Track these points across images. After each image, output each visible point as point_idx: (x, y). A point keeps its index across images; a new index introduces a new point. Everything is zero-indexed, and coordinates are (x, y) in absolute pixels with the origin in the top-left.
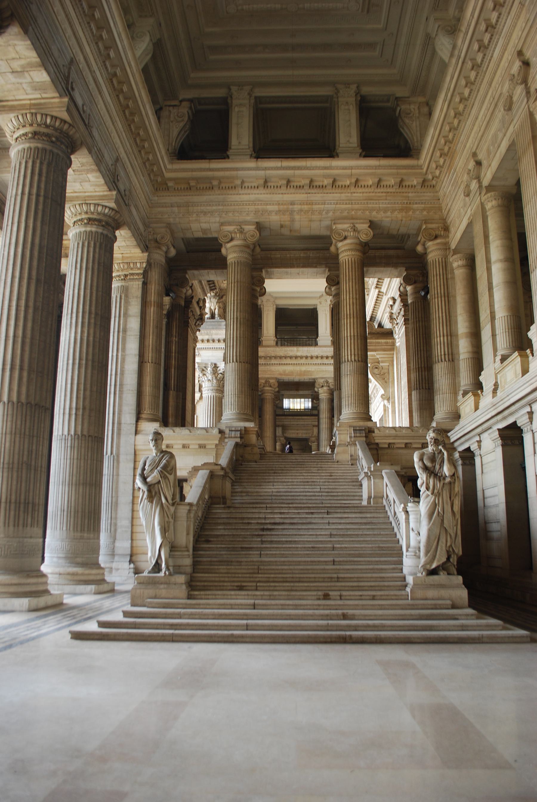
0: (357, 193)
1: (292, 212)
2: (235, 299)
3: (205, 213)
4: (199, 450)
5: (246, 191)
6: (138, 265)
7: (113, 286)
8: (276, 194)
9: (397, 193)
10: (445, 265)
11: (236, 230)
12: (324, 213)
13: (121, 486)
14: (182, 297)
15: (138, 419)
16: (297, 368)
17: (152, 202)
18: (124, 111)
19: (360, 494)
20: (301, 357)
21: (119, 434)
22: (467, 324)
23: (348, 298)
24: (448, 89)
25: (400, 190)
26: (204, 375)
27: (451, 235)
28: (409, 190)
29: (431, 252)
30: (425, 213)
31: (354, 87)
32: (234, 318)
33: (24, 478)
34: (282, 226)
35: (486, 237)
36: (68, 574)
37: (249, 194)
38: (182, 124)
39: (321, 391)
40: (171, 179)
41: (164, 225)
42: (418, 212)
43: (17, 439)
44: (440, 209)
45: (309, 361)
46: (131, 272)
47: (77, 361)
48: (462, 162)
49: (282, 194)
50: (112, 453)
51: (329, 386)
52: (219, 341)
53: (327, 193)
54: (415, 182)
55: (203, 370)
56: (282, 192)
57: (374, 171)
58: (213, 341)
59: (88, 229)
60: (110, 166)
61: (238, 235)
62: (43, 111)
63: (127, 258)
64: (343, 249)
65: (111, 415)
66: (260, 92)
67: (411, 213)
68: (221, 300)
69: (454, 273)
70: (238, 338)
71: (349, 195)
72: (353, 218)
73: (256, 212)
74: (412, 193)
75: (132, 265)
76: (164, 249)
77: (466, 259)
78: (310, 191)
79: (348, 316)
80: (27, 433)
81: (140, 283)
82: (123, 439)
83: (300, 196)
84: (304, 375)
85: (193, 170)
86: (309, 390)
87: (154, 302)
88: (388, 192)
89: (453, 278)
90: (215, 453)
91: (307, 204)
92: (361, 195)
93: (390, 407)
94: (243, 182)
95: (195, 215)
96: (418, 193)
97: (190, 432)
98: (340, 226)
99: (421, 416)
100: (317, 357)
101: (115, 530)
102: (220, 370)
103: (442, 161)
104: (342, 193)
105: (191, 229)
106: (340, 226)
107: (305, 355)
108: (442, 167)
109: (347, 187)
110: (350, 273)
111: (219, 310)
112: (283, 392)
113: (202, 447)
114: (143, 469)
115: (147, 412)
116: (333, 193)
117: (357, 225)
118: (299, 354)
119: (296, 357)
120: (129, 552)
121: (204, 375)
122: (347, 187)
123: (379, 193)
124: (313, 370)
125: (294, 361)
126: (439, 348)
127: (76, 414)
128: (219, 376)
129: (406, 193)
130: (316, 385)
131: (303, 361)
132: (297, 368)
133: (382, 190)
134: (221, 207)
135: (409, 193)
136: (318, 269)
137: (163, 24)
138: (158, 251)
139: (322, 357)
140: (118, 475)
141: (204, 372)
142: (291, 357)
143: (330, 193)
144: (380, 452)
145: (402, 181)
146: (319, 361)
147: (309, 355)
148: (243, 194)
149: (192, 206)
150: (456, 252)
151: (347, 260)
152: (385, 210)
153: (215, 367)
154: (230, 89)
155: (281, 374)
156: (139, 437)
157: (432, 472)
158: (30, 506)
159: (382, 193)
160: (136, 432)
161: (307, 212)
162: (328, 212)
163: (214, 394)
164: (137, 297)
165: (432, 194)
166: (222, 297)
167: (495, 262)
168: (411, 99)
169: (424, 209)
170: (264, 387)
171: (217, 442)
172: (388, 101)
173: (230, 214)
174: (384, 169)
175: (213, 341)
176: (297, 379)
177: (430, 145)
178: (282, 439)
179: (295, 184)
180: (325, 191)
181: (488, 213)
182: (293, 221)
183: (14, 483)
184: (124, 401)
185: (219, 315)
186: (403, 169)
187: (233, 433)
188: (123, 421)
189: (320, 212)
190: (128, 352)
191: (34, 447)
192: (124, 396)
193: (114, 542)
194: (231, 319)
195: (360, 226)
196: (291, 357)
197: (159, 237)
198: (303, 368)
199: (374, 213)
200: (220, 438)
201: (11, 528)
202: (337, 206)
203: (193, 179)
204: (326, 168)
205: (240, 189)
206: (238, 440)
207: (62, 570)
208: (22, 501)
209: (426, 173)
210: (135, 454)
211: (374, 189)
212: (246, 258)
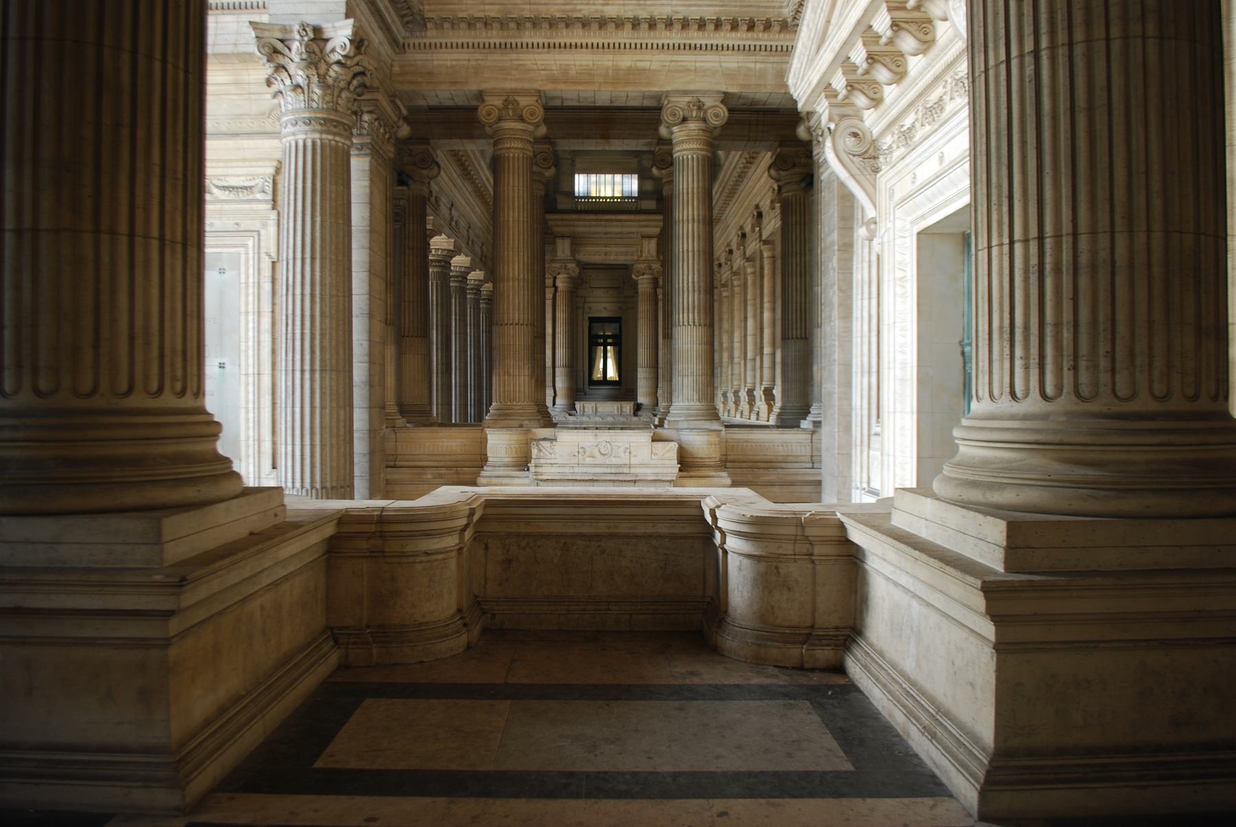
16: (607, 60)
19: (818, 478)
20: (619, 23)
26: (280, 68)
39: (678, 133)
51: (704, 120)
55: (276, 51)
84: (627, 83)
86: (638, 137)
100: (669, 23)
102: (333, 50)
107: (630, 15)
112: (567, 145)
119: (602, 23)
124: (655, 66)
125: (595, 37)
128: (332, 73)
130: (666, 116)
131: (625, 36)
132: (607, 60)
139: (685, 24)
141: (281, 60)
142: (585, 23)
146: (675, 37)
147: (643, 14)
153: (317, 37)
155: (554, 80)
163: (317, 136)
170: (500, 119)
176: (603, 95)
178: (572, 266)
196: (585, 23)
198: (626, 61)
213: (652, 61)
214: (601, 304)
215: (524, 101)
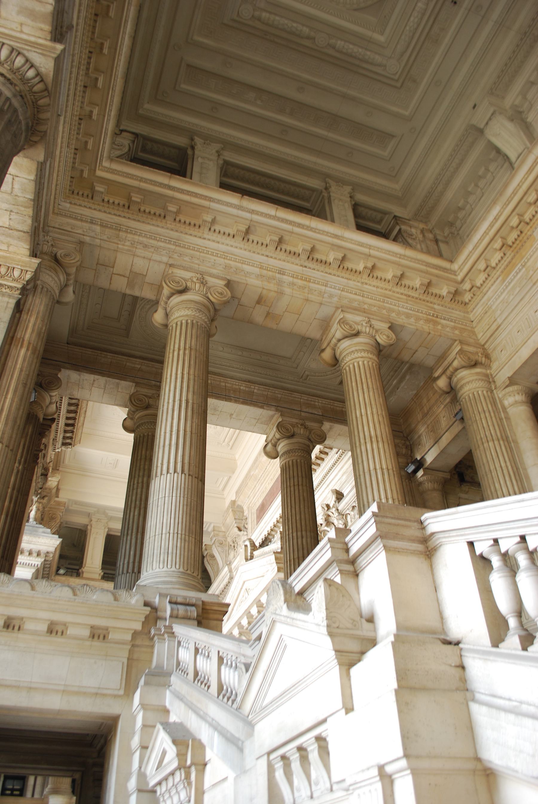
0: (370, 285)
1: (280, 283)
2: (186, 372)
4: (88, 643)
5: (215, 237)
6: (16, 273)
8: (258, 254)
9: (420, 299)
11: (195, 280)
12: (326, 295)
14: (42, 407)
17: (60, 207)
23: (369, 413)
28: (435, 301)
30: (457, 332)
32: (180, 400)
34: (260, 301)
37: (218, 242)
40: (103, 180)
41: (74, 240)
42: (448, 329)
49: (267, 256)
53: (330, 274)
56: (267, 253)
57: (398, 259)
61: (197, 285)
67: (439, 327)
68: (42, 501)
70: (188, 434)
71: (359, 284)
74: (439, 305)
77: (526, 394)
78: (306, 264)
79: (374, 439)
81: (12, 303)
83: (291, 266)
85: (141, 180)
87: (29, 343)
88: (409, 296)
90: (126, 654)
91: (302, 279)
92: (375, 289)
94: (214, 221)
95: (128, 243)
96: (446, 307)
97: (75, 594)
104: (350, 279)
105: (113, 267)
109: (358, 273)
110: (369, 381)
111: (36, 512)
113: (98, 634)
116: (338, 276)
122: (358, 273)
123: (398, 293)
129: (431, 303)
133: (402, 291)
135: (435, 304)
136: (265, 411)
143: (335, 275)
145: (429, 284)
148: (209, 240)
149: (126, 232)
151: (361, 363)
152: (408, 316)
154: (192, 140)
159: (402, 294)
161: (304, 288)
162: (331, 296)
165: (462, 314)
166: (43, 498)
168: (411, 222)
169: (454, 328)
171: (138, 626)
173: (186, 259)
174: (410, 261)
177: (486, 233)
179: (288, 248)
180: (327, 270)
182: (281, 293)
185: (35, 519)
186: (434, 268)
187: (181, 607)
189: (321, 294)
194: (174, 401)
195: (378, 325)
197: (60, 253)
199: (393, 315)
200: (147, 617)
202: (343, 293)
203: (140, 190)
204: (336, 236)
205: (207, 229)
209: (463, 280)
211: (393, 287)
212: (206, 322)
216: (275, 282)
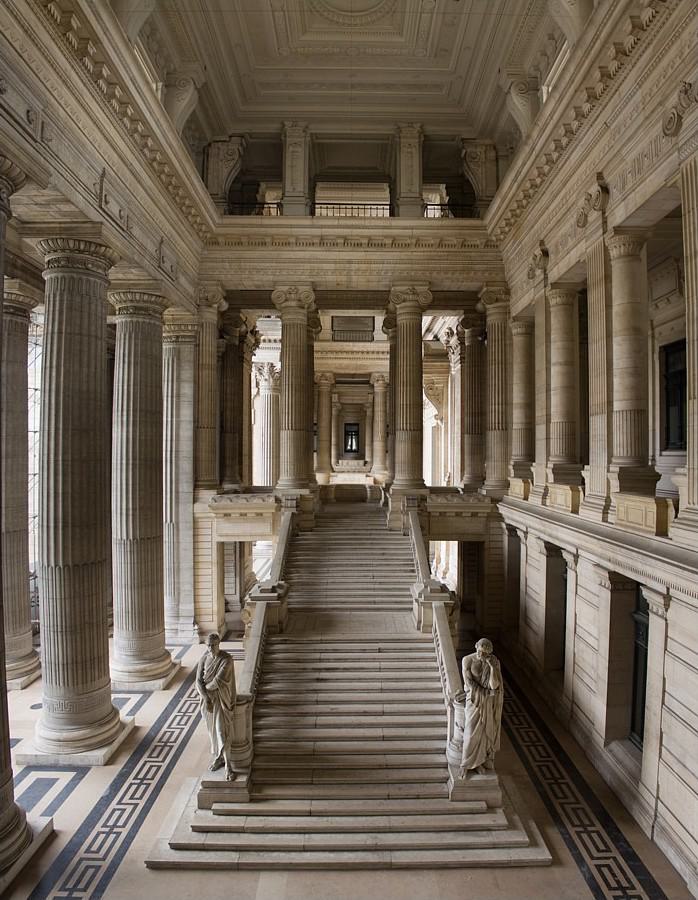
3: (258, 271)
5: (301, 248)
6: (190, 328)
7: (164, 347)
10: (505, 331)
13: (182, 552)
15: (196, 487)
18: (167, 188)
21: (177, 503)
22: (522, 395)
24: (519, 173)
25: (463, 249)
27: (512, 301)
29: (490, 315)
30: (486, 274)
31: (417, 126)
33: (87, 637)
35: (548, 334)
36: (137, 672)
38: (232, 164)
42: (479, 274)
43: (77, 602)
44: (502, 270)
45: (366, 356)
46: (182, 334)
47: (131, 462)
48: (528, 239)
50: (171, 521)
52: (275, 341)
54: (478, 242)
58: (270, 341)
59: (135, 320)
60: (154, 254)
62: (75, 237)
63: (178, 319)
64: (401, 311)
65: (169, 453)
66: (315, 128)
67: (472, 274)
69: (511, 339)
72: (411, 280)
73: (312, 270)
75: (183, 327)
76: (216, 306)
80: (86, 594)
82: (181, 508)
89: (512, 345)
93: (442, 460)
98: (398, 288)
99: (472, 460)
100: (373, 352)
101: (179, 594)
103: (507, 229)
106: (398, 288)
108: (506, 233)
114: (202, 674)
115: (204, 477)
117: (416, 288)
118: (355, 349)
119: (353, 352)
120: (193, 614)
121: (261, 374)
125: (351, 356)
126: (493, 418)
127: (133, 515)
131: (360, 355)
132: (354, 362)
133: (443, 249)
134: (274, 264)
137: (208, 67)
138: (211, 310)
139: (378, 352)
140: (178, 542)
142: (347, 352)
144: (432, 519)
146: (375, 356)
150: (515, 319)
152: (446, 271)
154: (284, 126)
155: (336, 368)
156: (197, 505)
157: (479, 684)
158: (96, 660)
160: (195, 501)
162: (387, 272)
164: (189, 361)
167: (555, 364)
172: (453, 140)
175: (270, 341)
181: (552, 309)
183: (79, 644)
184: (181, 471)
188: (181, 490)
190: (182, 418)
191: (94, 605)
192: (181, 462)
193: (178, 605)
195: (419, 289)
196: (347, 352)
197: (210, 295)
198: (359, 362)
199: (435, 274)
201: (80, 686)
206: (294, 510)
207: (131, 668)
208: (88, 659)
210: (194, 522)
213: (368, 362)
214: (350, 419)
215: (328, 374)
216: (345, 272)
